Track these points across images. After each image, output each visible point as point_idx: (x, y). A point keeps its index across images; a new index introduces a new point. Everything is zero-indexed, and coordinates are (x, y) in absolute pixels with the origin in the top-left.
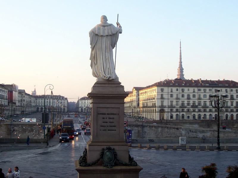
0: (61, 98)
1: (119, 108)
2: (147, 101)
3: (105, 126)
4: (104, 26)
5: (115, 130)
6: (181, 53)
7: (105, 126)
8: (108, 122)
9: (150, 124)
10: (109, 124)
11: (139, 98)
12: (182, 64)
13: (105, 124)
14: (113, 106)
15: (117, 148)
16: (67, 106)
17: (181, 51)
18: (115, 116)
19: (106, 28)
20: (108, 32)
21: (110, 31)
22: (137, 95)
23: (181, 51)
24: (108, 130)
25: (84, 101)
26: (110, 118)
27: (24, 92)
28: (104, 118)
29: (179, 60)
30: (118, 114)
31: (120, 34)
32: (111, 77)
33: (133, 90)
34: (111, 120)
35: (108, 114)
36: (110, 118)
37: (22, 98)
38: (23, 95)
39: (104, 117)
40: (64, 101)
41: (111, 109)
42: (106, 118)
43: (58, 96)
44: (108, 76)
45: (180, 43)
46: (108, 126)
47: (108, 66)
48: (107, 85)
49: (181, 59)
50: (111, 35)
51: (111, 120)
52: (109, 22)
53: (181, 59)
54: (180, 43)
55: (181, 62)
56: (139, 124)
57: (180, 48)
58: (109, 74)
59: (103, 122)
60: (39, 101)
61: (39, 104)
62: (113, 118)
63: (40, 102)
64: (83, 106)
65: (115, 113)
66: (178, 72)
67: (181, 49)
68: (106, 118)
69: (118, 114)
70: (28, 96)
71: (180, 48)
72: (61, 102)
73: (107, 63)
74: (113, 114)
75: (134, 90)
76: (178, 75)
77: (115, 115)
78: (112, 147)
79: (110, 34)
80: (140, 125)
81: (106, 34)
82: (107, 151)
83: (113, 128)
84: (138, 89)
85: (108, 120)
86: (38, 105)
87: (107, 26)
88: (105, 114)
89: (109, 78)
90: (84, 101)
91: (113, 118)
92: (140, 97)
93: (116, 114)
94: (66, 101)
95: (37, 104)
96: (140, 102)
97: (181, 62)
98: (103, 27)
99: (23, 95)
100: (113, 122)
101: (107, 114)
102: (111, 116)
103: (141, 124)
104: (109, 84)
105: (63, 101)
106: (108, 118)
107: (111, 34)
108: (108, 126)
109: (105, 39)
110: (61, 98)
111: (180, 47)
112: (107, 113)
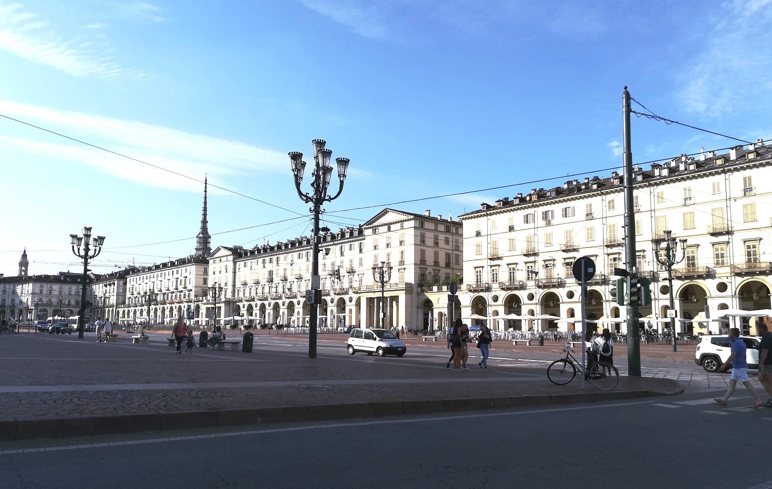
6: (205, 203)
12: (209, 225)
17: (206, 197)
23: (206, 197)
29: (201, 218)
45: (206, 180)
49: (205, 215)
53: (205, 215)
54: (206, 180)
55: (205, 222)
57: (206, 191)
66: (198, 242)
67: (206, 194)
71: (206, 191)
76: (197, 249)
97: (205, 222)
111: (204, 189)
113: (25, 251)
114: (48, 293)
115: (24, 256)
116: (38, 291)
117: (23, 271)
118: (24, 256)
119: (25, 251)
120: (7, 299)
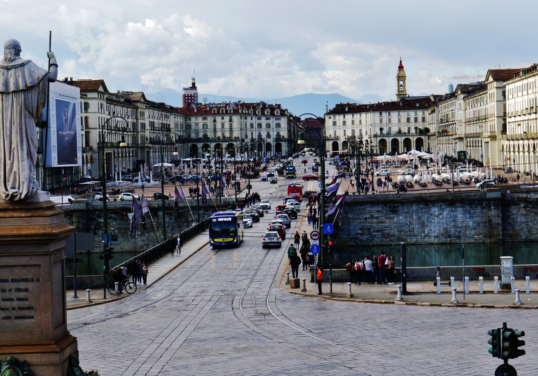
0: (267, 112)
1: (39, 265)
2: (526, 118)
3: (8, 309)
4: (8, 69)
5: (32, 317)
7: (8, 309)
8: (15, 299)
9: (529, 196)
10: (16, 304)
11: (505, 105)
13: (8, 304)
14: (24, 260)
15: (32, 359)
16: (286, 136)
18: (30, 286)
19: (12, 72)
20: (16, 83)
21: (20, 80)
22: (502, 98)
24: (16, 318)
25: (339, 118)
26: (18, 290)
27: (142, 100)
28: (4, 291)
30: (38, 280)
31: (51, 84)
32: (17, 196)
33: (487, 79)
34: (22, 295)
35: (13, 281)
36: (18, 290)
37: (137, 119)
38: (139, 110)
39: (5, 288)
40: (278, 121)
41: (19, 268)
42: (10, 290)
43: (258, 104)
44: (11, 192)
46: (14, 309)
47: (15, 169)
48: (7, 214)
50: (22, 90)
51: (22, 295)
52: (24, 56)
56: (489, 195)
58: (13, 188)
59: (3, 300)
60: (197, 124)
61: (197, 134)
62: (27, 290)
63: (201, 127)
64: (340, 134)
65: (30, 277)
68: (10, 290)
69: (38, 280)
70: (156, 112)
72: (268, 126)
73: (13, 160)
74: (26, 280)
75: (491, 79)
77: (30, 281)
78: (21, 358)
79: (21, 89)
80: (494, 199)
81: (12, 88)
82: (7, 369)
83: (27, 313)
84: (503, 76)
85: (15, 295)
86: (193, 136)
87: (15, 67)
88: (6, 281)
89: (13, 196)
90: (342, 117)
91: (27, 290)
92: (507, 102)
93: (32, 280)
94: (283, 122)
95: (189, 135)
96: (508, 120)
98: (5, 71)
99: (137, 108)
100: (26, 299)
101: (12, 280)
102: (22, 285)
103: (496, 195)
104: (14, 210)
105: (273, 122)
106: (13, 291)
107: (24, 88)
108: (14, 309)
109: (11, 100)
110: (267, 112)
112: (11, 277)
113: (401, 62)
114: (388, 122)
115: (401, 67)
116: (378, 121)
117: (401, 86)
118: (401, 67)
119: (401, 62)
120: (355, 129)
